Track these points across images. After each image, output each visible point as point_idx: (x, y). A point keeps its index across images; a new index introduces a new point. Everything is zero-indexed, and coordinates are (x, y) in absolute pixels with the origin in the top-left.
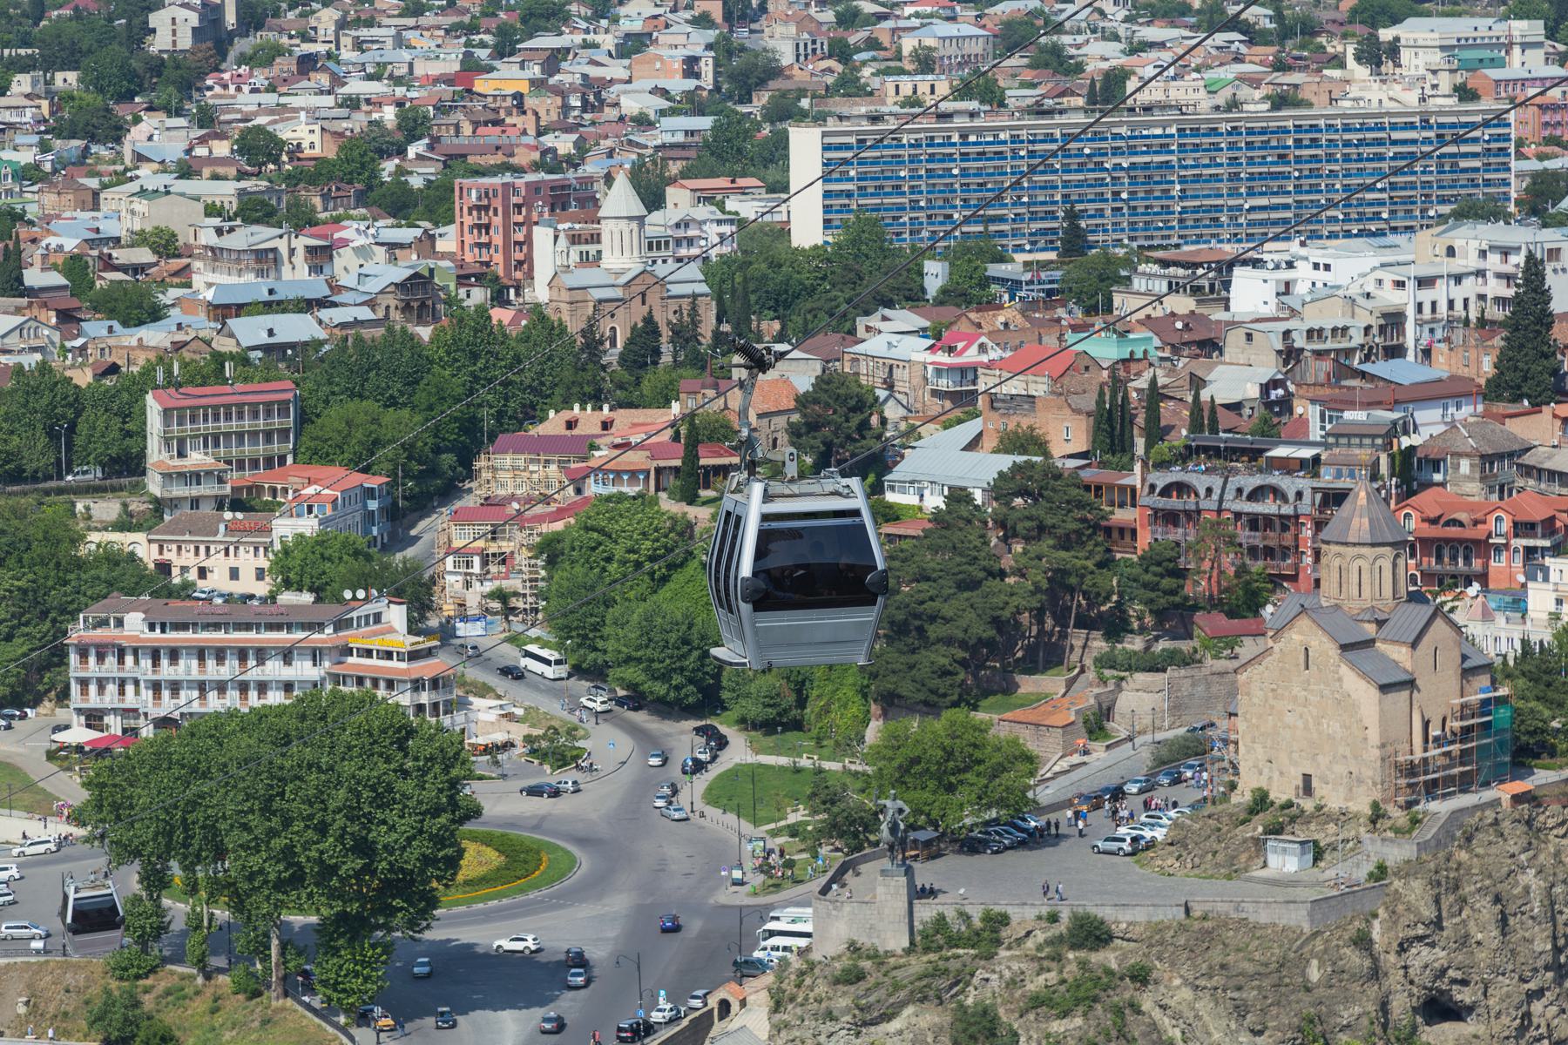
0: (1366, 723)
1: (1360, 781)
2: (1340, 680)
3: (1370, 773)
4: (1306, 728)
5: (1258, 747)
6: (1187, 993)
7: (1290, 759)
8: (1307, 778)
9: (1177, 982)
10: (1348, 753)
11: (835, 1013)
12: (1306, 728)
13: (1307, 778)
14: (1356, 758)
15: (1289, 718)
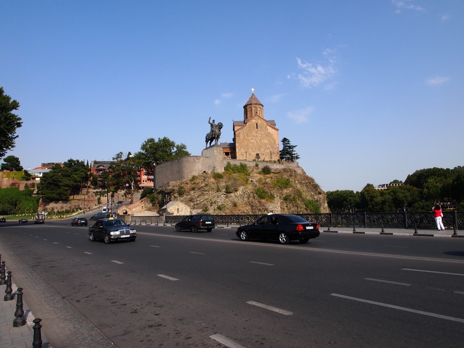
0: (275, 139)
1: (274, 153)
2: (267, 129)
3: (277, 151)
4: (257, 142)
5: (242, 150)
6: (299, 186)
7: (252, 151)
8: (258, 155)
9: (297, 182)
10: (270, 147)
11: (220, 188)
12: (257, 142)
13: (258, 155)
14: (272, 148)
15: (252, 141)
